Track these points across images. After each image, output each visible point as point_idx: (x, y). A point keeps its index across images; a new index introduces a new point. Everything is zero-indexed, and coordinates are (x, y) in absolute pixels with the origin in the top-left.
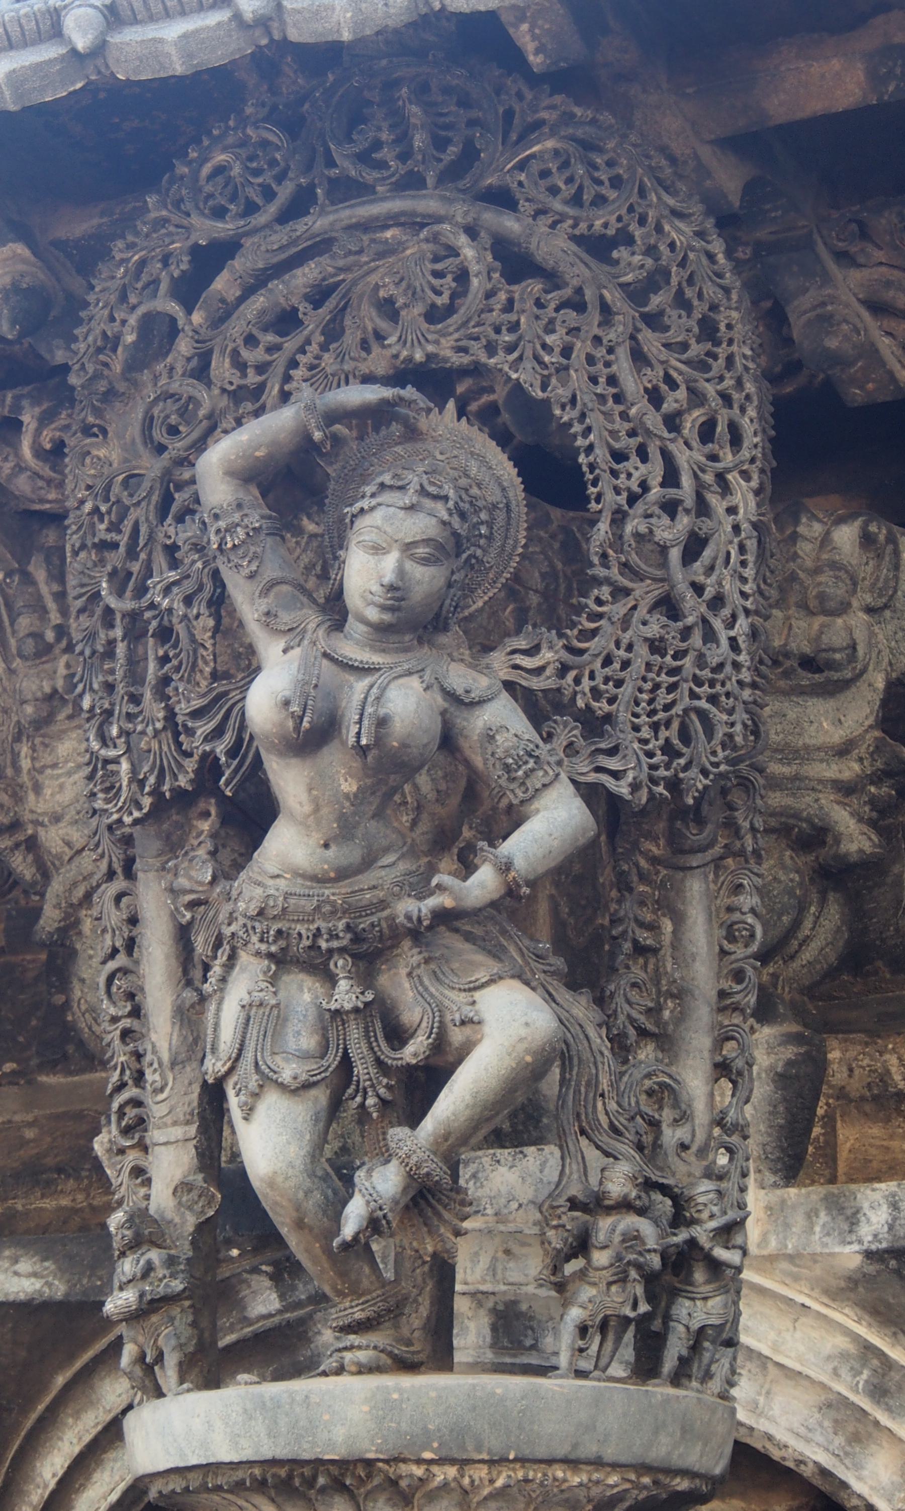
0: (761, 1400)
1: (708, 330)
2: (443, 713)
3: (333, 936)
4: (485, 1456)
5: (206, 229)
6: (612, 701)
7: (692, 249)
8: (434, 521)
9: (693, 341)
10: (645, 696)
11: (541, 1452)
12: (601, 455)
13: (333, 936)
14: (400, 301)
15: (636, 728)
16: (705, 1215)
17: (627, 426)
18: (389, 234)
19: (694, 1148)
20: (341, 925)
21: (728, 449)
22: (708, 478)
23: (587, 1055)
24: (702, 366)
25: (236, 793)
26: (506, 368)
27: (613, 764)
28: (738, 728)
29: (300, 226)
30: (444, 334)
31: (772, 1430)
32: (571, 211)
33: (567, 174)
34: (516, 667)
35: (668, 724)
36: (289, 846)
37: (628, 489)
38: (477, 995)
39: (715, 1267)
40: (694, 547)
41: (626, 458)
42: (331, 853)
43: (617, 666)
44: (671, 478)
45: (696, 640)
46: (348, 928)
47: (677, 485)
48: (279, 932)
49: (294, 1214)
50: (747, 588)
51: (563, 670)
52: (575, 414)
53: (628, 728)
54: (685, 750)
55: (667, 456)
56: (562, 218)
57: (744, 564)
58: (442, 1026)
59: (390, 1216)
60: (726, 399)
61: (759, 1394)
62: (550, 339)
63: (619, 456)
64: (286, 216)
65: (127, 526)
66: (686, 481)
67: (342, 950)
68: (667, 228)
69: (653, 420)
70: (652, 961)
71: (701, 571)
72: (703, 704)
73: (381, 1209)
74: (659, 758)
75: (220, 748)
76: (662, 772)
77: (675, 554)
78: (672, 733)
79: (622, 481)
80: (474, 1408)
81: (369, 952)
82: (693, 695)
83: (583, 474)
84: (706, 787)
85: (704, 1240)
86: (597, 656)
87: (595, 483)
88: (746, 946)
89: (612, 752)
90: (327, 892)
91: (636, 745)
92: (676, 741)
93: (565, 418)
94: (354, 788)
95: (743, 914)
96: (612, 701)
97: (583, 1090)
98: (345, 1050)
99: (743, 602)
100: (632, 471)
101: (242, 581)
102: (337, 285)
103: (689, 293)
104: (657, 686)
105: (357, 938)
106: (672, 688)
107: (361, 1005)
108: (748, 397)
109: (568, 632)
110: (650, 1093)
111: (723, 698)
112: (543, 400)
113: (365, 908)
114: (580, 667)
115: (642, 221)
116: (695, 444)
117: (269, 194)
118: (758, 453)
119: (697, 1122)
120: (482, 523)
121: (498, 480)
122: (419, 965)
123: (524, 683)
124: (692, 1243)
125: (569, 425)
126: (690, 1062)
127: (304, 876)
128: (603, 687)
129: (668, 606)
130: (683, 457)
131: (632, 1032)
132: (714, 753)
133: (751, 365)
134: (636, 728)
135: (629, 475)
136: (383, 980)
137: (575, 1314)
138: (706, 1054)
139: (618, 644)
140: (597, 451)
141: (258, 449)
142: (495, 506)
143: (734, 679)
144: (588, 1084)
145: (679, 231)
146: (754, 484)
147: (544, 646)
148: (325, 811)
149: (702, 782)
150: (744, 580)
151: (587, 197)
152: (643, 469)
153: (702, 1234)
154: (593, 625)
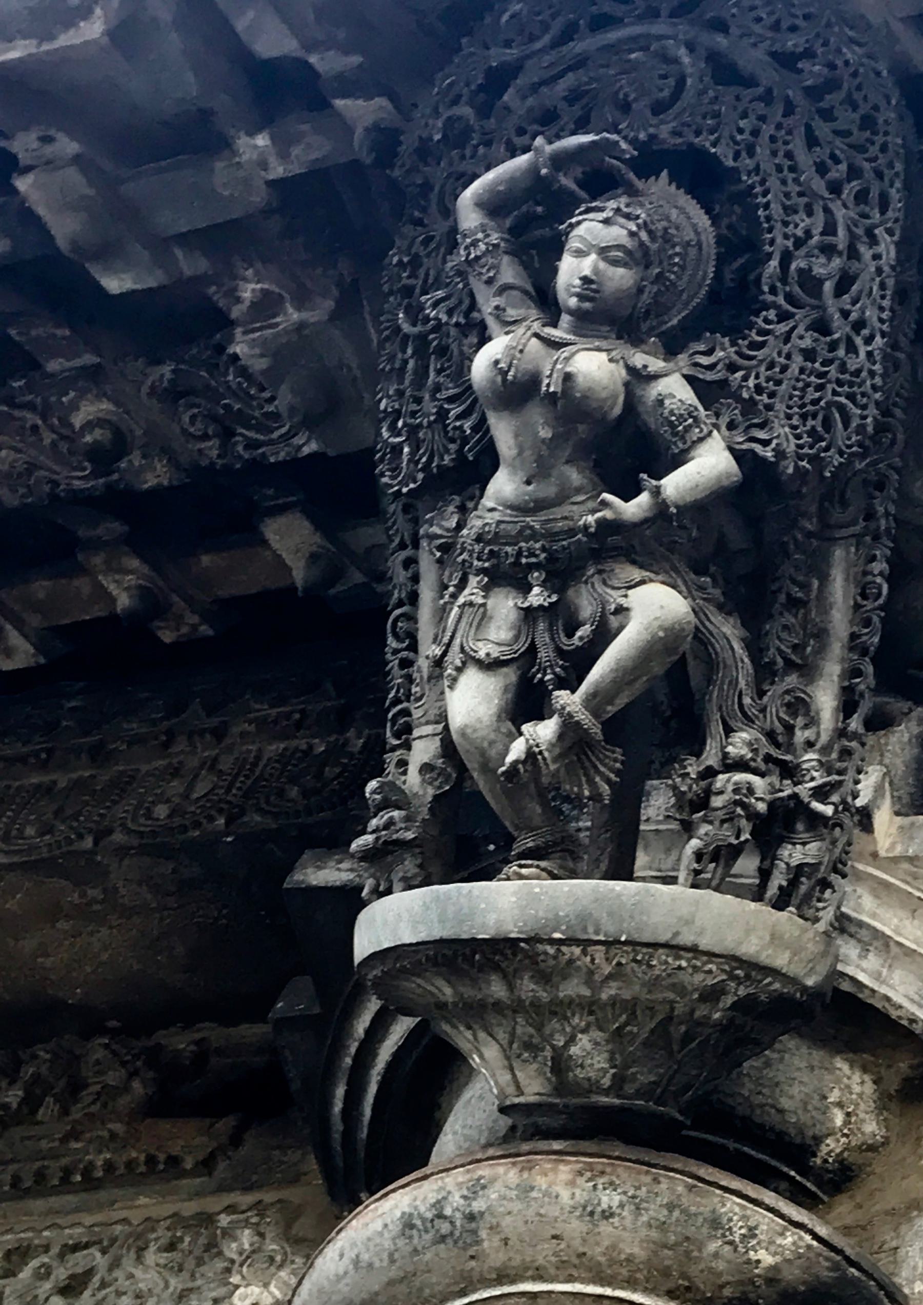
0: (885, 972)
1: (868, 123)
2: (627, 385)
3: (532, 554)
4: (601, 938)
5: (498, 56)
6: (772, 395)
7: (862, 65)
8: (625, 232)
9: (855, 132)
10: (797, 393)
11: (646, 937)
12: (776, 210)
13: (532, 554)
14: (632, 96)
15: (789, 417)
16: (807, 778)
17: (798, 189)
18: (633, 56)
19: (818, 746)
20: (538, 545)
21: (877, 210)
22: (860, 231)
23: (730, 662)
24: (860, 149)
25: (476, 457)
26: (707, 144)
27: (762, 435)
28: (869, 420)
29: (564, 49)
30: (663, 122)
31: (891, 994)
32: (770, 34)
33: (768, 9)
34: (696, 365)
35: (814, 417)
36: (503, 485)
37: (794, 235)
38: (630, 592)
39: (816, 821)
40: (844, 284)
41: (796, 212)
42: (531, 488)
43: (777, 370)
44: (830, 229)
45: (841, 352)
46: (543, 549)
47: (834, 233)
48: (491, 551)
49: (481, 760)
50: (885, 315)
51: (732, 368)
52: (757, 178)
53: (782, 415)
54: (826, 436)
55: (826, 210)
56: (763, 39)
57: (883, 297)
58: (603, 615)
59: (546, 754)
60: (880, 175)
61: (883, 966)
62: (742, 124)
63: (790, 210)
64: (557, 43)
65: (422, 272)
66: (841, 232)
67: (537, 566)
68: (845, 50)
69: (819, 185)
70: (802, 611)
71: (849, 301)
72: (843, 400)
73: (537, 746)
74: (806, 439)
75: (467, 425)
76: (806, 450)
77: (828, 286)
78: (817, 423)
79: (790, 229)
80: (597, 900)
81: (563, 571)
82: (835, 393)
83: (761, 223)
84: (841, 464)
85: (805, 795)
86: (761, 361)
87: (770, 231)
88: (876, 600)
89: (761, 426)
90: (528, 519)
91: (787, 429)
92: (819, 429)
93: (750, 182)
94: (550, 435)
95: (875, 576)
96: (772, 395)
97: (725, 687)
98: (533, 639)
99: (879, 325)
100: (798, 221)
101: (483, 287)
102: (587, 92)
103: (857, 96)
104: (808, 385)
105: (552, 558)
106: (820, 388)
107: (546, 604)
108: (897, 174)
109: (740, 341)
110: (789, 705)
111: (859, 396)
112: (733, 168)
113: (557, 534)
114: (749, 369)
115: (825, 44)
116: (851, 204)
117: (546, 27)
118: (900, 215)
119: (822, 727)
120: (677, 254)
121: (695, 227)
122: (593, 575)
123: (701, 376)
124: (795, 796)
125: (752, 187)
126: (821, 683)
127: (511, 507)
128: (764, 385)
129: (821, 327)
130: (840, 214)
131: (779, 660)
132: (849, 439)
133: (902, 151)
134: (789, 417)
135: (796, 226)
136: (571, 593)
137: (695, 843)
138: (836, 678)
139: (779, 354)
140: (772, 206)
141: (500, 184)
142: (688, 244)
143: (868, 383)
144: (730, 683)
145: (854, 52)
146: (896, 238)
147: (718, 349)
148: (527, 453)
149: (837, 460)
150: (882, 309)
151: (784, 25)
152: (808, 221)
153: (804, 790)
154: (761, 339)
